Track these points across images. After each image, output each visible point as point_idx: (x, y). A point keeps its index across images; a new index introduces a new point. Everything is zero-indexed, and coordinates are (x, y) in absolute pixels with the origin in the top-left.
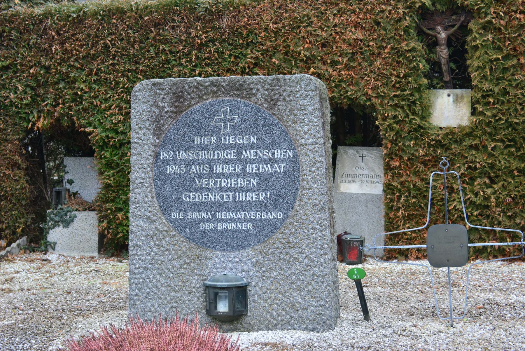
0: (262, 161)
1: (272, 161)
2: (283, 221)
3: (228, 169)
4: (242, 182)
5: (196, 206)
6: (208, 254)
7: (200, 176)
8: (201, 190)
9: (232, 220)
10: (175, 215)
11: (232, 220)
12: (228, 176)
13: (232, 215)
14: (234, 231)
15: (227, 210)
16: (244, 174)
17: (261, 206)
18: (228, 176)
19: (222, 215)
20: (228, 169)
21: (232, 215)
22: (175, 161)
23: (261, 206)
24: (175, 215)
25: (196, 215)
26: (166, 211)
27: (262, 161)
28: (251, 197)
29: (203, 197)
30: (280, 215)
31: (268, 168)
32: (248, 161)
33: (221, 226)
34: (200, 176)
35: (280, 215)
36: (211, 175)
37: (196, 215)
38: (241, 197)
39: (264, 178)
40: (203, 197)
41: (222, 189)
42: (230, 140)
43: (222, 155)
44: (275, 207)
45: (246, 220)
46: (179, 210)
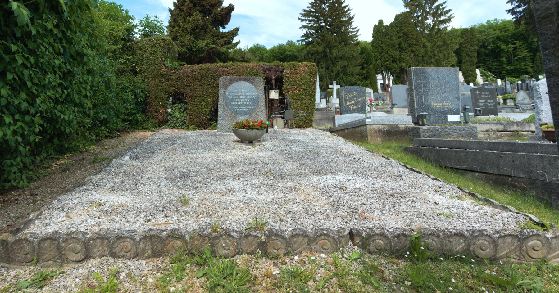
0: (250, 95)
1: (253, 95)
2: (255, 109)
3: (242, 97)
4: (245, 100)
5: (234, 105)
6: (237, 116)
7: (236, 99)
8: (236, 102)
9: (243, 109)
10: (230, 107)
11: (243, 109)
12: (242, 99)
13: (243, 107)
14: (244, 111)
15: (242, 106)
16: (246, 98)
17: (250, 105)
18: (242, 99)
19: (241, 107)
20: (242, 97)
21: (243, 107)
22: (230, 95)
23: (250, 105)
24: (230, 107)
25: (234, 107)
26: (227, 106)
27: (250, 95)
28: (248, 103)
29: (236, 103)
30: (254, 107)
31: (252, 97)
32: (247, 95)
33: (240, 110)
34: (236, 99)
35: (254, 107)
36: (238, 98)
37: (234, 107)
38: (245, 103)
39: (251, 99)
40: (236, 103)
41: (241, 101)
42: (243, 91)
43: (241, 94)
44: (253, 106)
45: (246, 109)
46: (230, 106)
